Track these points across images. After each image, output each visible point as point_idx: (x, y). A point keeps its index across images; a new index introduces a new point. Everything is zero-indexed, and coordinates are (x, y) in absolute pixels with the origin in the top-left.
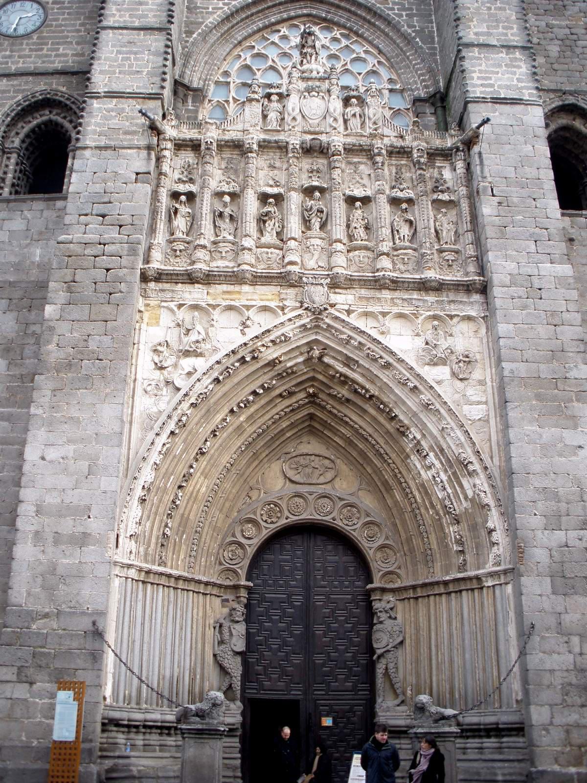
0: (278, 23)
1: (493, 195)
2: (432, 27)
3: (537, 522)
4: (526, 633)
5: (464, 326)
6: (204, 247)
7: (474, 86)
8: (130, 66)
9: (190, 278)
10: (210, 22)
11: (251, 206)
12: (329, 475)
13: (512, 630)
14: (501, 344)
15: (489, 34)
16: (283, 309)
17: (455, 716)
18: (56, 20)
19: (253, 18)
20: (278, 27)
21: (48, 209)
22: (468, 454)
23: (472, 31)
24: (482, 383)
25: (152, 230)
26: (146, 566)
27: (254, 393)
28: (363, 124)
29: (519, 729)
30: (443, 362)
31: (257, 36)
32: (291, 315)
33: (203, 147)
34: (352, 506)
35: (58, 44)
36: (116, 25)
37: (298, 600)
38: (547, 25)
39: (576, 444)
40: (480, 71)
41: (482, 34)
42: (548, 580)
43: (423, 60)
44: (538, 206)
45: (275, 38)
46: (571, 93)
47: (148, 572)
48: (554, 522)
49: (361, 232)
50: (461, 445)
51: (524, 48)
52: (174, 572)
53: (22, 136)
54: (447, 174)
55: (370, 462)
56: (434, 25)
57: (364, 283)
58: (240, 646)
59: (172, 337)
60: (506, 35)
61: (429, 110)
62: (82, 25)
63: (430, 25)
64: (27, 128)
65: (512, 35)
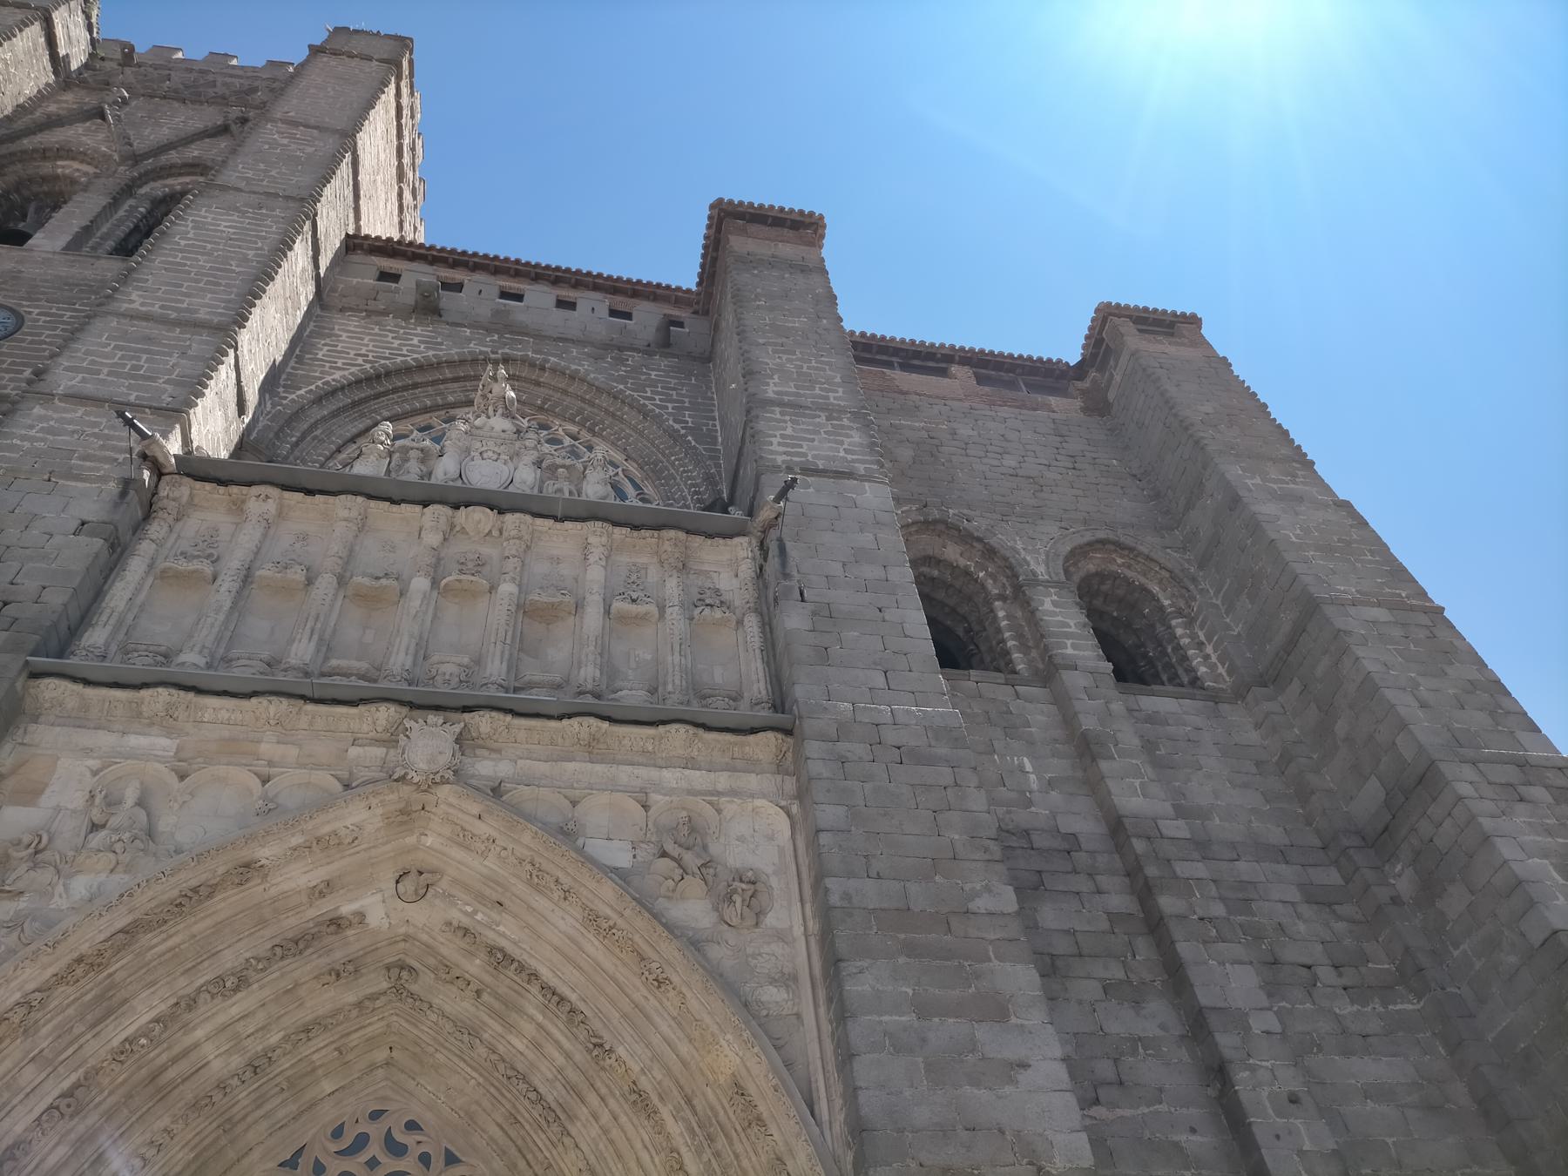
1: (803, 601)
2: (715, 425)
7: (772, 452)
10: (334, 380)
14: (822, 842)
19: (417, 391)
31: (421, 420)
35: (24, 365)
40: (782, 436)
41: (787, 394)
44: (887, 618)
56: (717, 423)
63: (711, 422)
65: (835, 398)
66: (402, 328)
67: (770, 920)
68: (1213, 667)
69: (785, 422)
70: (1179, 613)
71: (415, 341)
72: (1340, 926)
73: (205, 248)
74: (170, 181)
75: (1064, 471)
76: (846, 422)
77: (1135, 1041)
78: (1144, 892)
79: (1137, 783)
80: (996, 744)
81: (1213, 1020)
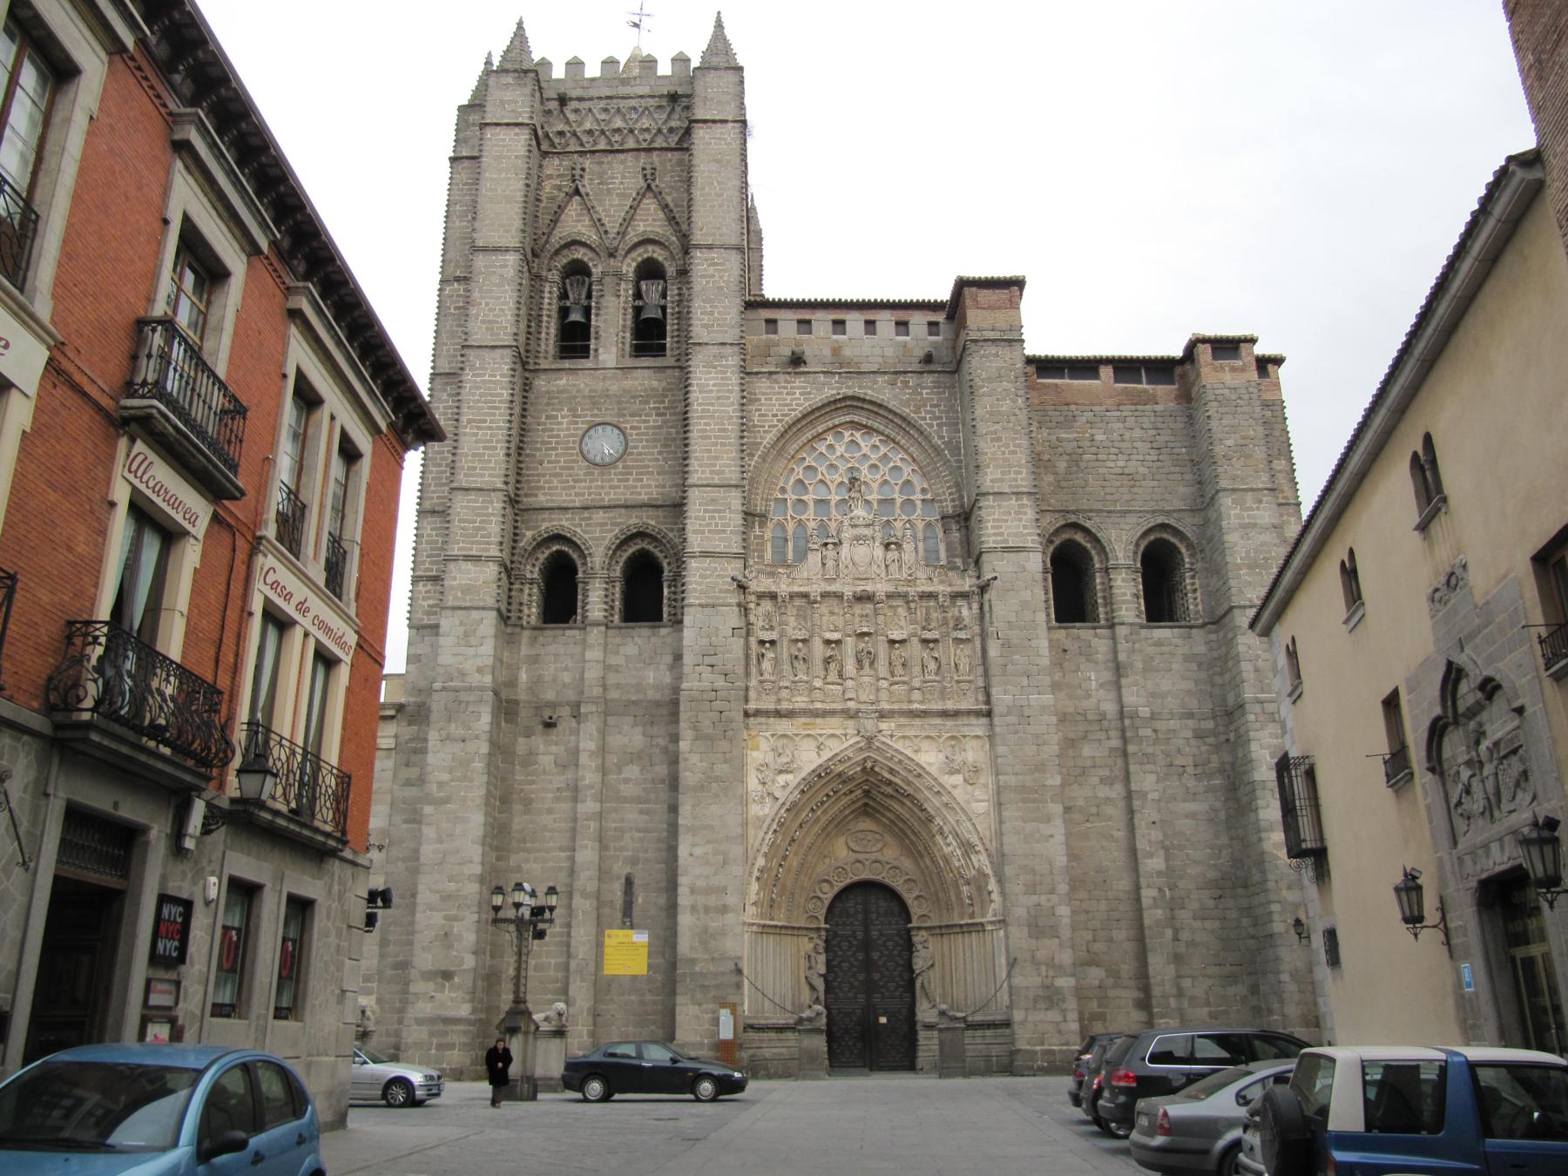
0: (825, 432)
3: (1019, 889)
4: (1012, 964)
5: (974, 743)
6: (787, 688)
7: (989, 535)
8: (716, 525)
9: (778, 714)
11: (818, 650)
12: (879, 846)
13: (1003, 961)
15: (1002, 480)
16: (845, 735)
17: (964, 1018)
18: (636, 447)
20: (824, 436)
21: (654, 635)
22: (974, 840)
23: (990, 478)
24: (985, 786)
25: (748, 674)
26: (763, 922)
27: (827, 795)
28: (900, 566)
29: (1007, 1024)
30: (958, 771)
31: (808, 447)
32: (852, 741)
33: (779, 599)
34: (896, 868)
35: (641, 474)
36: (700, 483)
37: (860, 935)
38: (1058, 439)
39: (1049, 833)
40: (994, 520)
42: (1026, 929)
43: (950, 474)
45: (822, 447)
46: (1074, 512)
47: (764, 926)
48: (1032, 889)
49: (899, 670)
50: (970, 833)
51: (1030, 494)
52: (780, 924)
53: (621, 564)
54: (965, 612)
55: (908, 837)
57: (902, 713)
58: (823, 970)
59: (770, 758)
60: (1016, 480)
61: (954, 527)
62: (660, 453)
64: (626, 555)
66: (789, 382)
67: (982, 780)
68: (1196, 605)
69: (993, 507)
70: (1191, 569)
71: (797, 395)
72: (1204, 748)
73: (708, 411)
74: (634, 254)
75: (1151, 464)
76: (1025, 501)
77: (1107, 799)
78: (1125, 740)
79: (1135, 689)
80: (1082, 667)
81: (1135, 796)
